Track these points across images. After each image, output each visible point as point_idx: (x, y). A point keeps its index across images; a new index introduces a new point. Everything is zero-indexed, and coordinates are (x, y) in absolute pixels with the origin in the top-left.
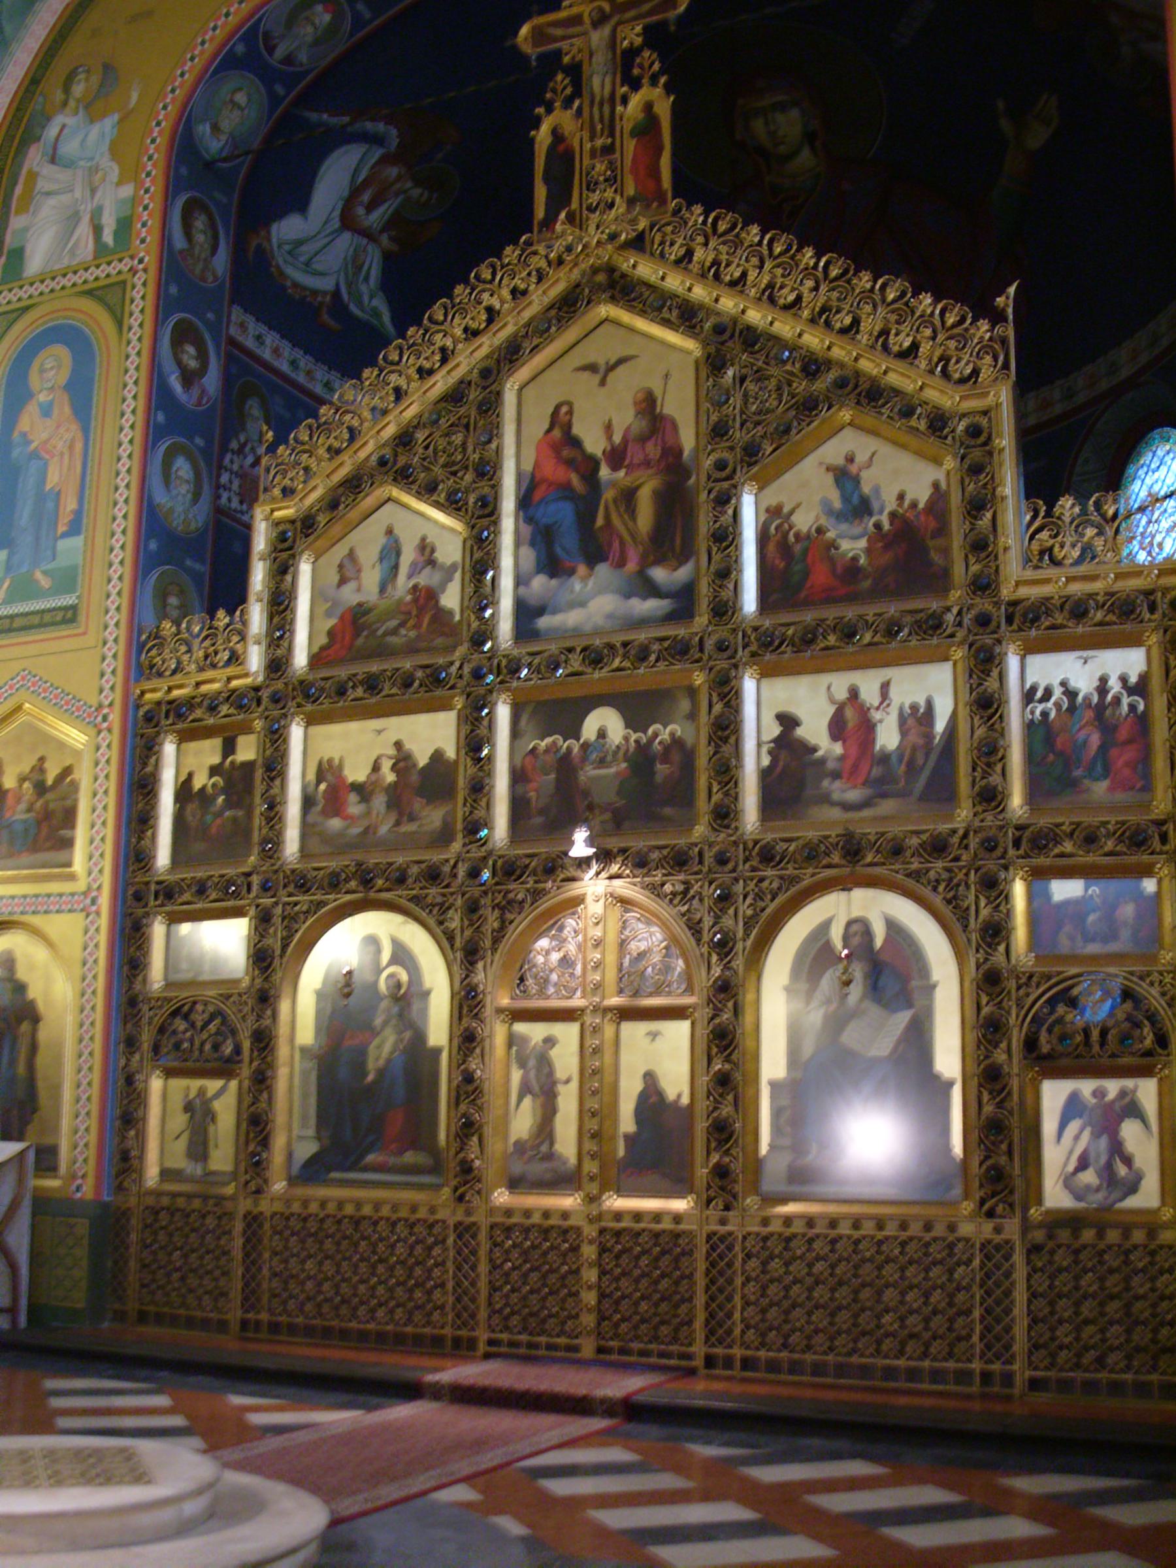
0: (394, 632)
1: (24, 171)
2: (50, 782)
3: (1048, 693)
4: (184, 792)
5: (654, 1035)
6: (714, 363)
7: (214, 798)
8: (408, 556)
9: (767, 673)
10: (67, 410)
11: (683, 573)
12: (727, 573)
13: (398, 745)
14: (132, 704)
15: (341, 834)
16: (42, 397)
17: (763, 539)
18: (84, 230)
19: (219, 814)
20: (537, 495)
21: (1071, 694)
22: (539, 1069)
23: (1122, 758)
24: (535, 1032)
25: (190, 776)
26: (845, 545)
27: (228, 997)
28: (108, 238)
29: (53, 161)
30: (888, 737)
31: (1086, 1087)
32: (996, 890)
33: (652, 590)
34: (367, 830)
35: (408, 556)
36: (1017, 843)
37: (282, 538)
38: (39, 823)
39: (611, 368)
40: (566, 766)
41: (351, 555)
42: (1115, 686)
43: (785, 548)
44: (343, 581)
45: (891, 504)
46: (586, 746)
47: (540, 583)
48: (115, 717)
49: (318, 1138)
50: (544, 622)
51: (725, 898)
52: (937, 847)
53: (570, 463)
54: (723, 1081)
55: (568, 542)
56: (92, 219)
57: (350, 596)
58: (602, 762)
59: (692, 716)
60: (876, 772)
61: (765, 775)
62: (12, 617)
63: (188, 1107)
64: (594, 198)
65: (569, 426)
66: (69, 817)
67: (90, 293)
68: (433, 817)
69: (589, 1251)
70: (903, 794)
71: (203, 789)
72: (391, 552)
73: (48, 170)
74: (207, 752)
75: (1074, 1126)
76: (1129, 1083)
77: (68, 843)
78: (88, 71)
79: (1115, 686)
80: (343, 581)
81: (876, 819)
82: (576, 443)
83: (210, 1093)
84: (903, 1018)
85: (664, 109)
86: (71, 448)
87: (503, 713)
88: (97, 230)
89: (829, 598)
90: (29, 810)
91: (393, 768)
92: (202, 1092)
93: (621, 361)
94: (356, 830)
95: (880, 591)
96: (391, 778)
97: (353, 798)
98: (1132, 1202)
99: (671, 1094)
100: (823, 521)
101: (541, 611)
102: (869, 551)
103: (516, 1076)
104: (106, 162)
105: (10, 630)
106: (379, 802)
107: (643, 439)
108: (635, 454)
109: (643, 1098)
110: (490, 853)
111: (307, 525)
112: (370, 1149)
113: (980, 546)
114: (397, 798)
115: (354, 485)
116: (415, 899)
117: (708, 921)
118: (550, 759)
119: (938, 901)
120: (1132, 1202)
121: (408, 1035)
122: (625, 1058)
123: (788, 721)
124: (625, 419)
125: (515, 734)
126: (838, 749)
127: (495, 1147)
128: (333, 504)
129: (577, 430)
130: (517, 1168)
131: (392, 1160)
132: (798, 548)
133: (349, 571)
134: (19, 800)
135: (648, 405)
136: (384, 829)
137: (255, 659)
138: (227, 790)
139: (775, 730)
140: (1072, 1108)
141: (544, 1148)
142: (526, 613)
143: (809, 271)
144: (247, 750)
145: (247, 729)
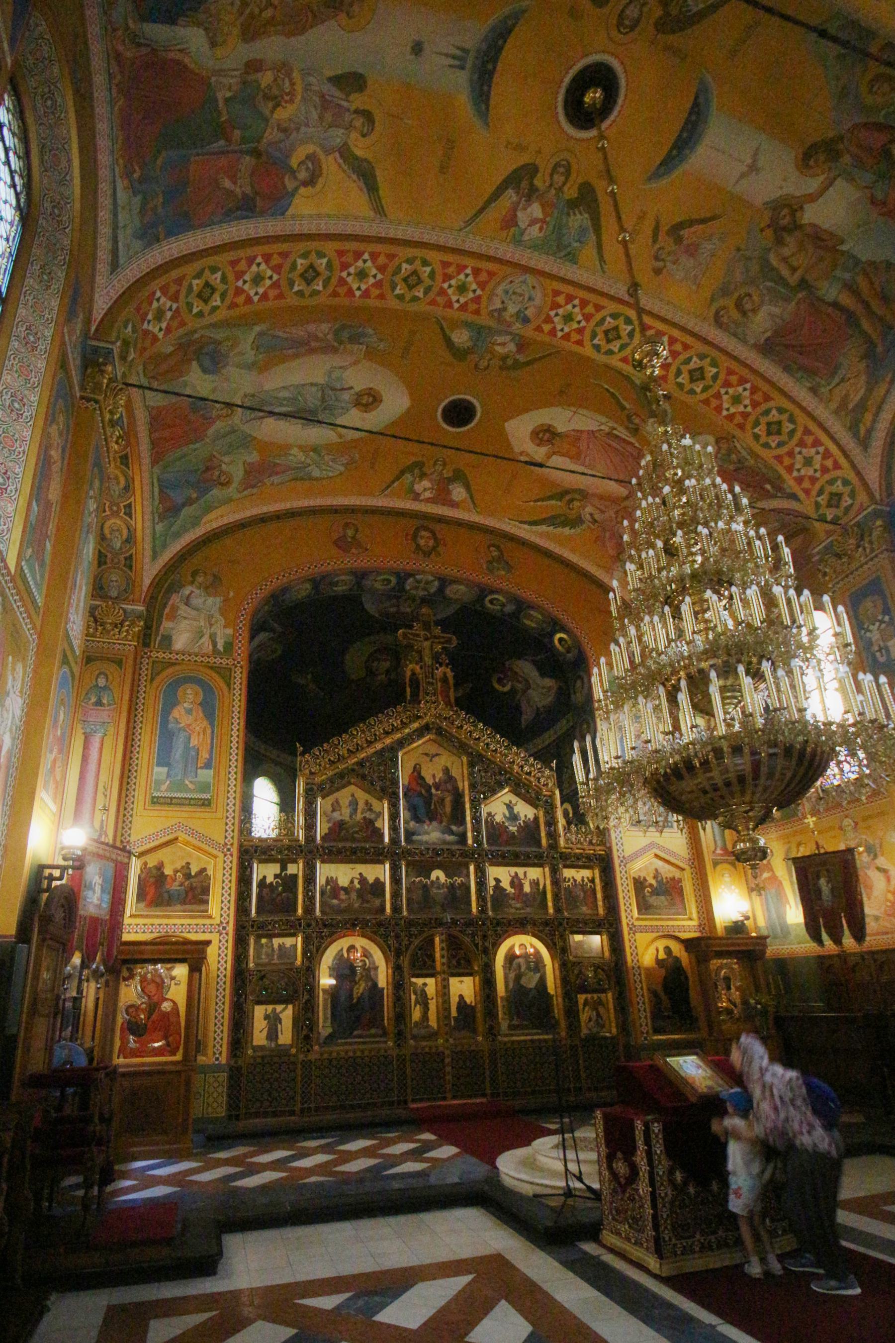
0: (357, 832)
1: (170, 603)
4: (262, 883)
5: (461, 982)
6: (471, 765)
7: (277, 888)
8: (361, 805)
10: (201, 715)
11: (461, 829)
13: (360, 874)
17: (486, 822)
18: (206, 640)
19: (280, 894)
21: (575, 881)
24: (419, 981)
25: (265, 877)
27: (291, 969)
28: (220, 647)
29: (187, 604)
30: (527, 889)
31: (589, 996)
32: (563, 937)
33: (452, 833)
35: (361, 805)
37: (311, 789)
38: (187, 893)
39: (433, 756)
41: (337, 801)
44: (334, 810)
45: (523, 818)
46: (432, 882)
47: (412, 824)
48: (235, 850)
50: (415, 838)
51: (485, 937)
53: (421, 786)
54: (488, 996)
55: (422, 811)
56: (210, 637)
57: (337, 816)
58: (438, 888)
59: (468, 876)
62: (171, 798)
63: (267, 1017)
64: (428, 698)
65: (419, 773)
66: (206, 890)
67: (211, 668)
68: (377, 902)
69: (447, 1060)
72: (354, 804)
73: (183, 607)
77: (207, 902)
78: (205, 573)
80: (334, 810)
82: (423, 778)
84: (538, 975)
85: (450, 674)
88: (215, 644)
89: (507, 843)
92: (274, 1010)
93: (437, 755)
94: (343, 905)
96: (358, 886)
97: (342, 892)
99: (468, 1001)
101: (413, 834)
104: (217, 615)
105: (171, 804)
106: (354, 895)
107: (446, 783)
108: (443, 787)
109: (459, 1003)
111: (321, 788)
113: (553, 836)
114: (361, 894)
115: (341, 775)
116: (375, 933)
121: (370, 984)
123: (498, 881)
124: (440, 775)
125: (407, 876)
128: (331, 780)
129: (423, 774)
130: (415, 1031)
131: (365, 1033)
134: (174, 880)
135: (446, 771)
136: (356, 905)
137: (301, 835)
138: (284, 884)
140: (586, 1003)
142: (409, 834)
143: (499, 742)
144: (292, 869)
145: (295, 861)
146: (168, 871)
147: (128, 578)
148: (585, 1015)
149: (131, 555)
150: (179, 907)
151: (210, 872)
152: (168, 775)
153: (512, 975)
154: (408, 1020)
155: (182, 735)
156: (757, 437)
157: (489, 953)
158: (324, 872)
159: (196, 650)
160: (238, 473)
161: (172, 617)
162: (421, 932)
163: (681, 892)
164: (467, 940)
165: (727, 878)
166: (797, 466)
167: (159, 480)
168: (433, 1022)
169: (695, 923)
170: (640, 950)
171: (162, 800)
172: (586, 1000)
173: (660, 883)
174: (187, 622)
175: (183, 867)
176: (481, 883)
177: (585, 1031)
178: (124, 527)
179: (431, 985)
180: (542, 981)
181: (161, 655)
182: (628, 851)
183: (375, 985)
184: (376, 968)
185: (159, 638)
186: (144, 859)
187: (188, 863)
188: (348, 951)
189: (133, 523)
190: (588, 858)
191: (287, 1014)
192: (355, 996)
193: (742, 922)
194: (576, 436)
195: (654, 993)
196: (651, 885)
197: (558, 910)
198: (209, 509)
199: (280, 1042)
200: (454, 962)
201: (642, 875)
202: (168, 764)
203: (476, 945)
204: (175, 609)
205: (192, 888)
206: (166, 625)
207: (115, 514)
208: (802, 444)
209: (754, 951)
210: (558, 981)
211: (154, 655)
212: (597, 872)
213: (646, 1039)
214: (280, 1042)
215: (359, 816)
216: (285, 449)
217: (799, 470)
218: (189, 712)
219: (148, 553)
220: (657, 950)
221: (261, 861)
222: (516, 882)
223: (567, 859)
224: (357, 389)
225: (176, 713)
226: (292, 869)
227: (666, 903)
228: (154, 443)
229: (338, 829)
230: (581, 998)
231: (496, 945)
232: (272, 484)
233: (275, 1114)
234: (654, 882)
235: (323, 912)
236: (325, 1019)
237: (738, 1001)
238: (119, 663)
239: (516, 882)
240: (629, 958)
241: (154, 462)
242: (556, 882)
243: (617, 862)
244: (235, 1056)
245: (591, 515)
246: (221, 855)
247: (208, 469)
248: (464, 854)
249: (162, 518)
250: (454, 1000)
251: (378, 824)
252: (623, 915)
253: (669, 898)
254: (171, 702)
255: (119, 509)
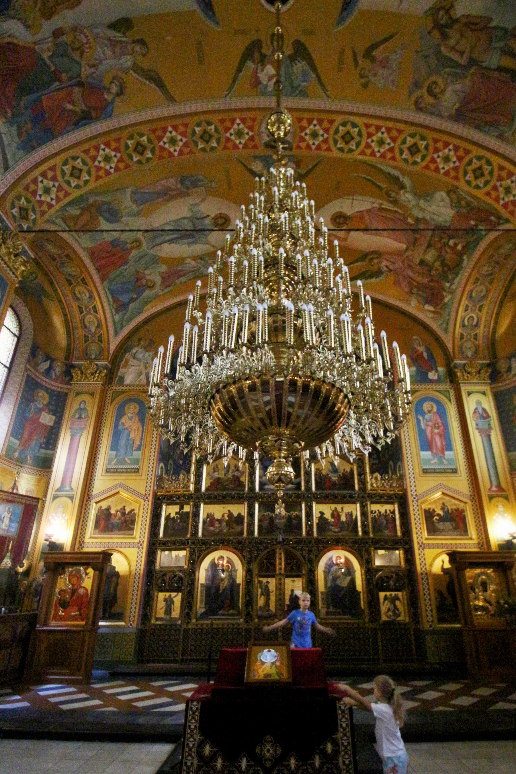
0: (228, 485)
2: (127, 512)
3: (375, 512)
4: (168, 518)
5: (294, 581)
9: (317, 503)
10: (137, 419)
12: (308, 482)
13: (229, 511)
14: (155, 494)
15: (214, 531)
16: (129, 415)
17: (315, 474)
19: (179, 524)
20: (264, 460)
21: (380, 513)
22: (265, 589)
23: (390, 526)
24: (264, 580)
25: (170, 514)
26: (333, 478)
30: (343, 518)
31: (388, 593)
34: (220, 531)
36: (372, 542)
38: (122, 523)
40: (272, 519)
42: (388, 512)
43: (320, 478)
44: (214, 471)
45: (342, 471)
48: (150, 498)
49: (205, 608)
51: (310, 551)
52: (355, 542)
57: (216, 475)
58: (280, 519)
59: (301, 510)
60: (341, 525)
61: (317, 524)
63: (165, 600)
66: (133, 522)
68: (239, 528)
70: (347, 530)
71: (174, 518)
73: (131, 360)
74: (176, 508)
75: (386, 602)
76: (396, 593)
77: (133, 529)
79: (388, 512)
80: (214, 471)
81: (343, 535)
83: (172, 596)
84: (349, 578)
86: (138, 429)
87: (257, 506)
90: (120, 519)
91: (228, 517)
92: (170, 596)
94: (218, 530)
95: (339, 489)
96: (227, 518)
98: (399, 619)
100: (329, 473)
101: (265, 485)
102: (338, 480)
103: (260, 591)
106: (224, 524)
110: (254, 538)
112: (221, 609)
114: (228, 523)
117: (307, 555)
118: (268, 518)
119: (357, 553)
120: (399, 619)
121: (231, 581)
122: (286, 586)
123: (322, 513)
125: (259, 511)
126: (333, 520)
127: (254, 607)
130: (260, 613)
132: (323, 478)
133: (216, 470)
137: (192, 488)
138: (181, 519)
139: (319, 515)
140: (386, 598)
141: (267, 608)
144: (187, 509)
145: (188, 504)
146: (113, 511)
147: (101, 348)
148: (384, 607)
149: (101, 335)
150: (117, 532)
151: (136, 511)
152: (116, 455)
153: (330, 577)
154: (254, 604)
155: (126, 432)
156: (468, 183)
157: (313, 563)
158: (204, 510)
159: (137, 383)
160: (158, 280)
161: (125, 366)
162: (266, 548)
163: (463, 520)
164: (298, 553)
165: (501, 508)
166: (502, 196)
167: (109, 290)
168: (272, 606)
169: (476, 541)
170: (428, 562)
171: (112, 470)
172: (386, 596)
173: (446, 513)
174: (133, 367)
175: (121, 509)
176: (309, 515)
177: (384, 618)
178: (95, 320)
179: (272, 583)
180: (353, 582)
181: (118, 388)
182: (420, 491)
183: (234, 581)
184: (236, 571)
185: (117, 379)
186: (99, 505)
187: (124, 507)
188: (218, 559)
189: (99, 316)
190: (390, 497)
191: (177, 598)
192: (221, 588)
193: (511, 540)
194: (360, 215)
195: (440, 593)
196: (439, 515)
197: (365, 532)
198: (146, 303)
199: (173, 616)
200: (289, 568)
201: (432, 507)
202: (117, 450)
203: (304, 557)
204: (127, 361)
205: (125, 521)
206: (122, 370)
207: (89, 313)
208: (500, 179)
209: (504, 562)
210: (364, 583)
211: (114, 388)
212: (396, 506)
213: (431, 626)
214: (173, 616)
215: (230, 475)
216: (182, 260)
217: (503, 199)
218: (130, 419)
219: (112, 332)
220: (443, 562)
221: (168, 504)
222: (336, 515)
223: (372, 497)
224: (213, 215)
225: (123, 420)
226: (187, 509)
227: (451, 527)
228: (99, 269)
229: (216, 484)
230: (382, 595)
231: (318, 558)
232: (181, 283)
233: (165, 662)
234: (441, 513)
235: (203, 535)
236: (201, 601)
237: (493, 601)
238: (92, 394)
239: (336, 515)
240: (419, 568)
241: (103, 279)
242: (364, 514)
243: (410, 499)
244: (143, 623)
245: (387, 266)
246: (142, 501)
247: (138, 280)
248: (298, 496)
249: (117, 311)
250: (288, 594)
251: (242, 479)
252: (415, 536)
253: (454, 524)
254: (120, 413)
255: (86, 309)
